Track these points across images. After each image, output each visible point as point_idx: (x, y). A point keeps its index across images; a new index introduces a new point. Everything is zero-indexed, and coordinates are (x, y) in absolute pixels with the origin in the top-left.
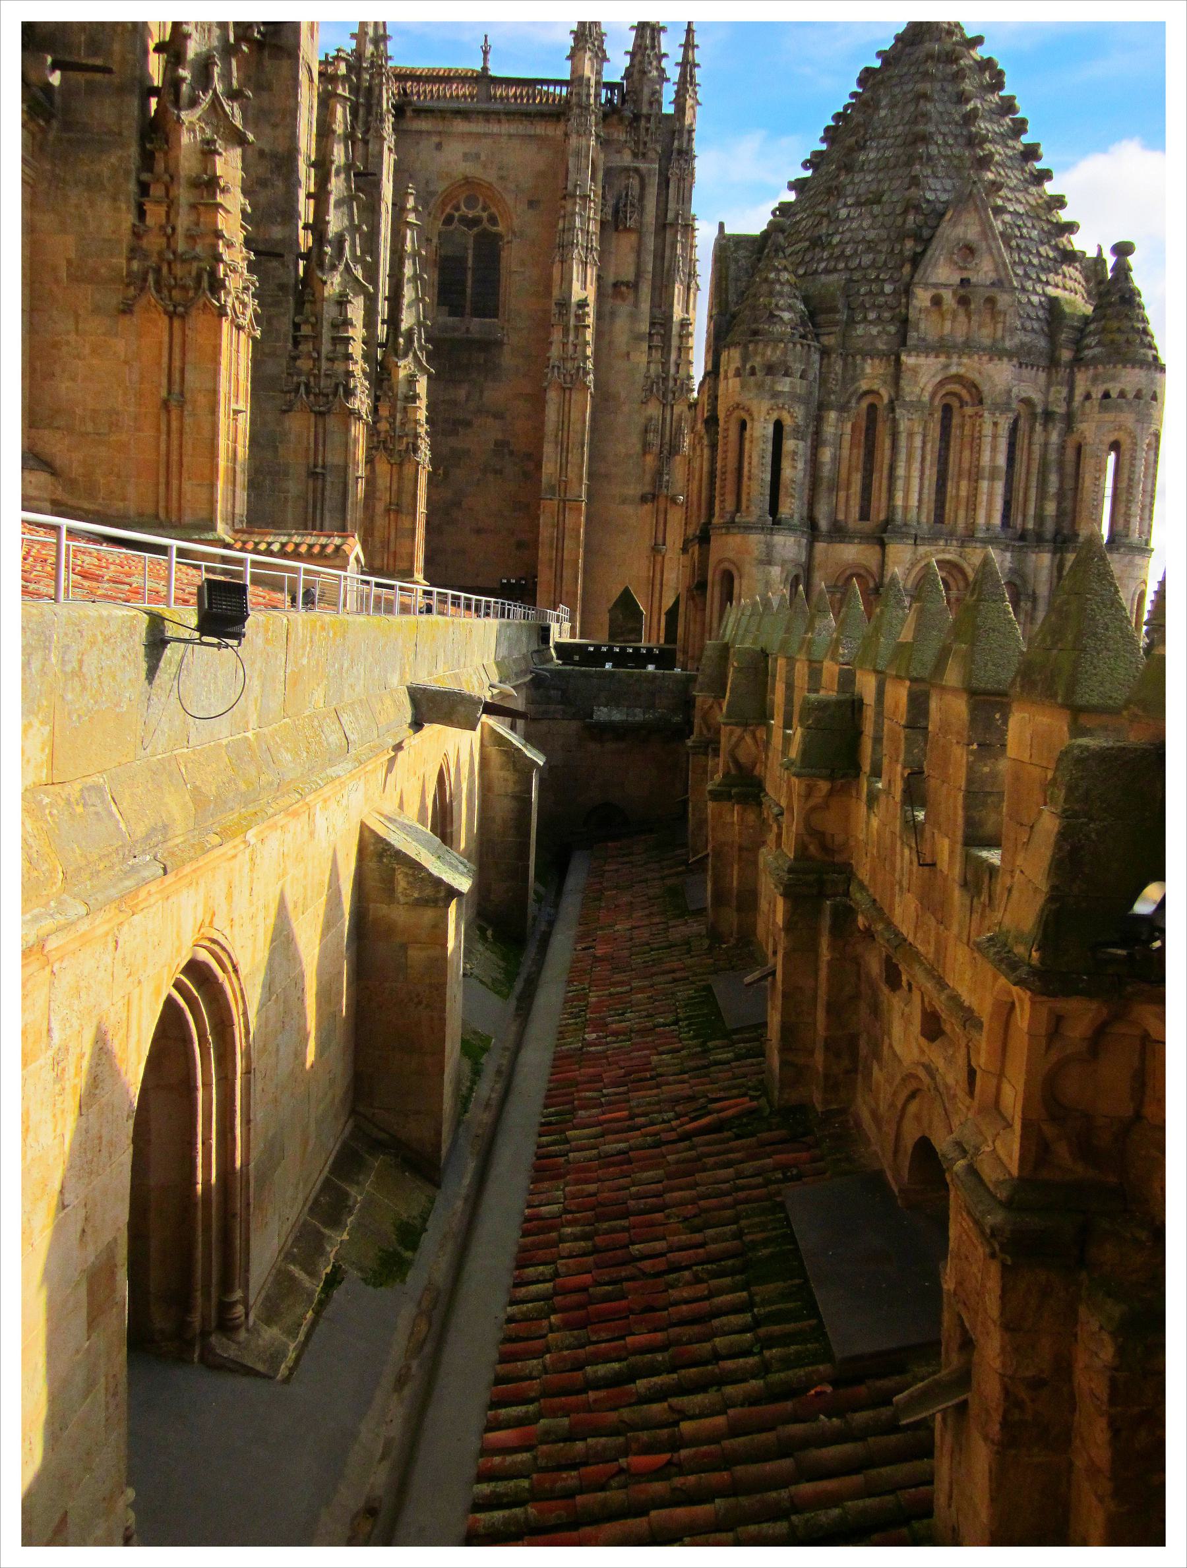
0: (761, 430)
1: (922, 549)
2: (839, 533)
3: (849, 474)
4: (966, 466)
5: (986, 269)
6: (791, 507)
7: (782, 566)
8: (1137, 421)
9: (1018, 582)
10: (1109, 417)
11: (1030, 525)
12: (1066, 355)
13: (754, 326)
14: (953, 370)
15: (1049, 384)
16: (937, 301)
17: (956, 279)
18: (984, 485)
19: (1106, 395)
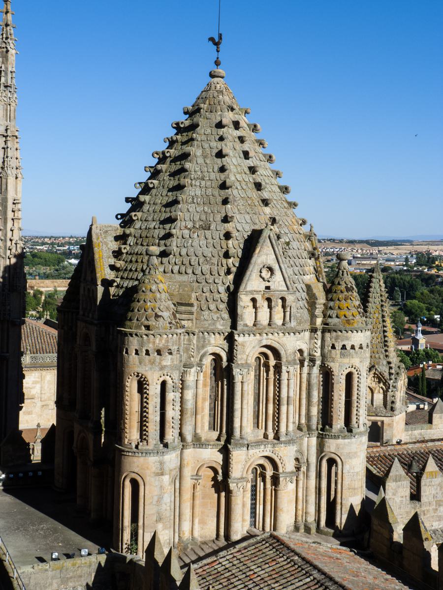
0: (154, 390)
1: (251, 452)
2: (198, 442)
3: (202, 403)
4: (271, 395)
5: (279, 280)
6: (171, 435)
7: (170, 474)
8: (361, 362)
9: (299, 457)
10: (346, 360)
11: (303, 421)
12: (319, 321)
13: (146, 323)
14: (265, 343)
15: (311, 338)
16: (254, 300)
17: (264, 285)
18: (284, 409)
19: (344, 347)
